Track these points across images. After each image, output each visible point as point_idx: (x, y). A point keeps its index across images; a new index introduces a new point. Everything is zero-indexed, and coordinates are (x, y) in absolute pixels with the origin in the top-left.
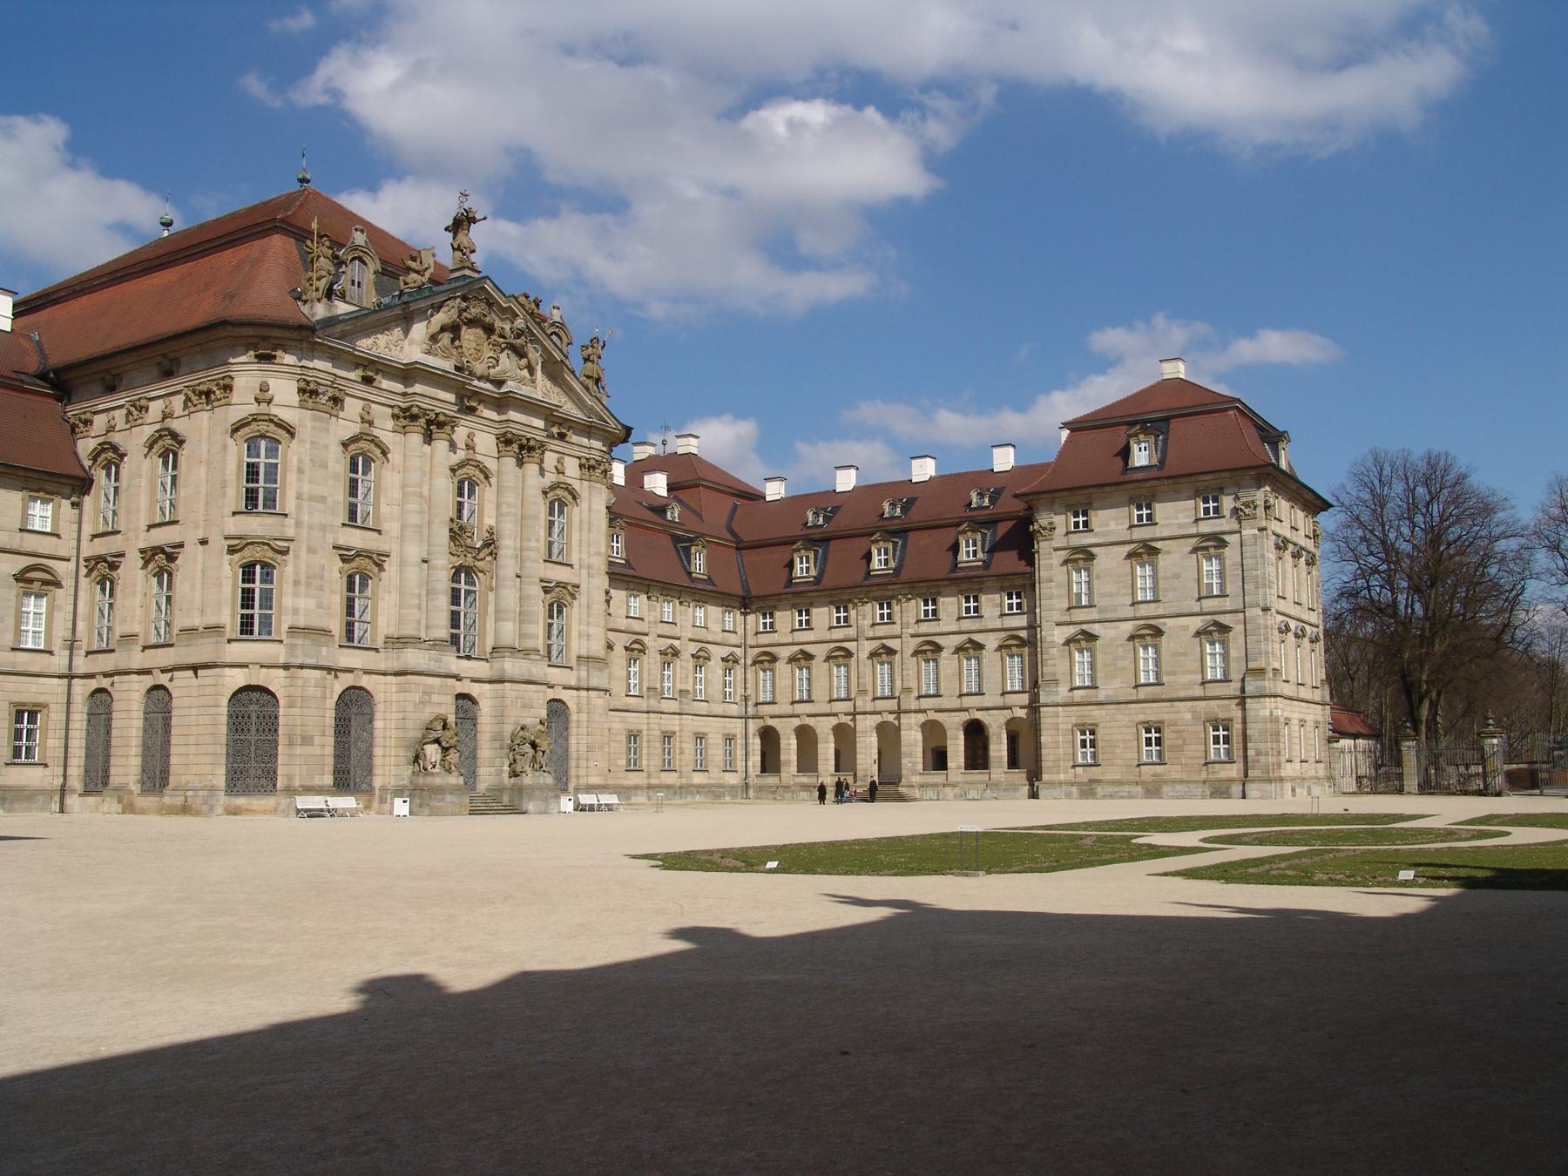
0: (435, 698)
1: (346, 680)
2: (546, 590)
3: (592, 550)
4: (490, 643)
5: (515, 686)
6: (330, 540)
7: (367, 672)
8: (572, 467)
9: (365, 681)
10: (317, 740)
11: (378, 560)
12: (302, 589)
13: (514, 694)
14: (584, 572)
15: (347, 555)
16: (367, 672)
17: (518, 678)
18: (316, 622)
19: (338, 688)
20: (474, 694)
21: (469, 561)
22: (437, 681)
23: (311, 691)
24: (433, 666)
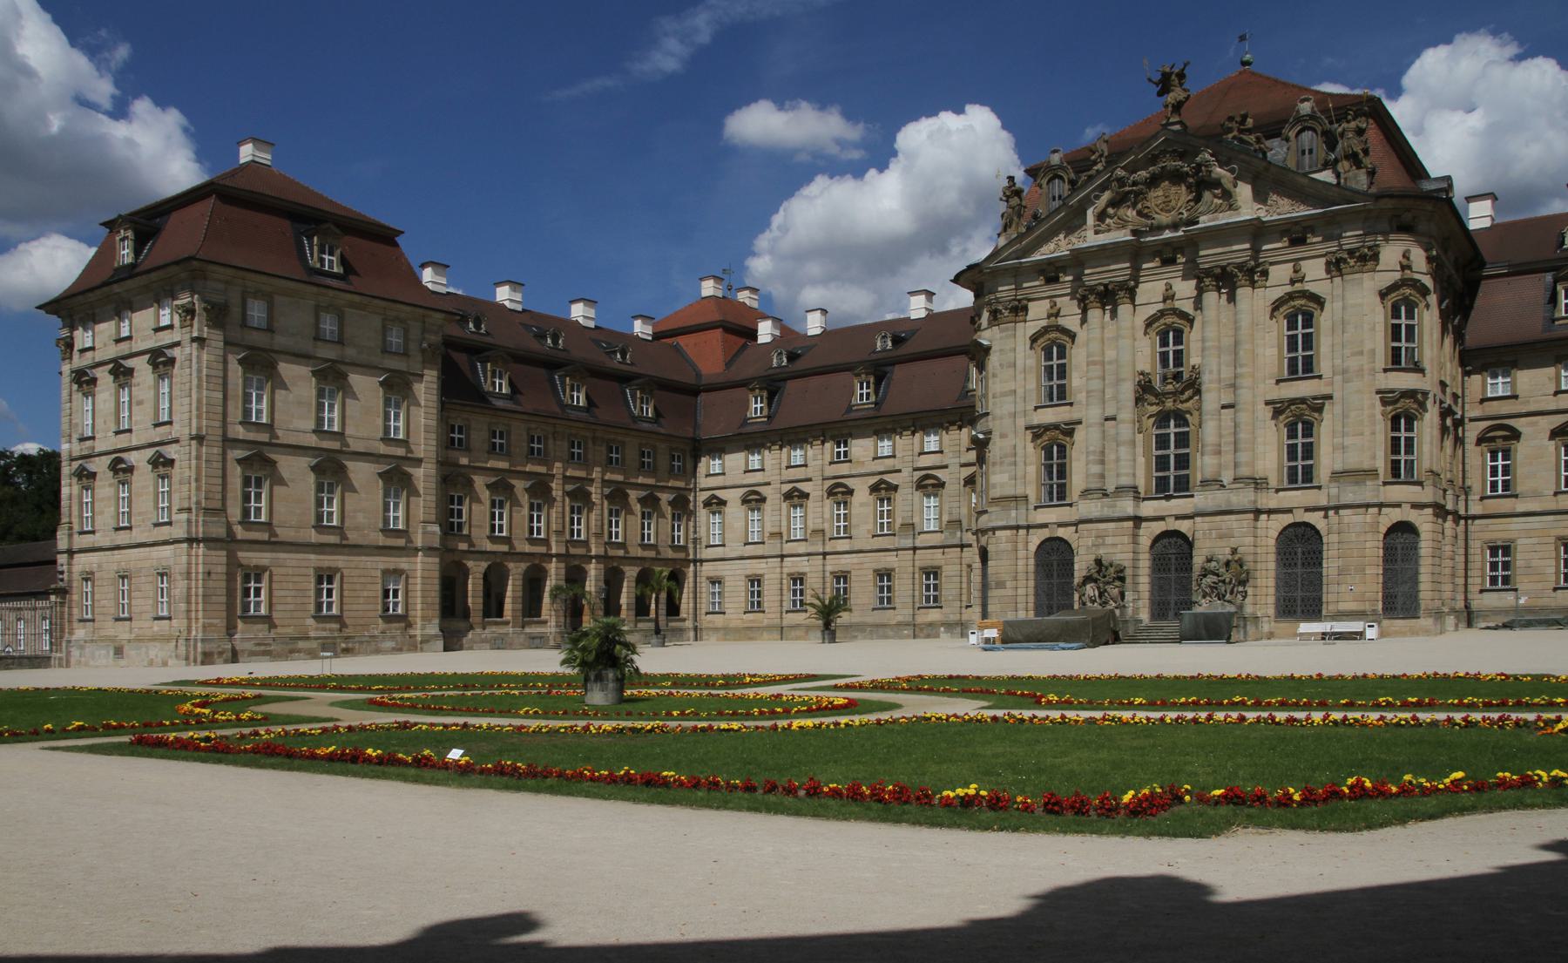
0: (1109, 540)
1: (1045, 534)
2: (1384, 402)
3: (1347, 352)
4: (1199, 478)
5: (1207, 519)
6: (1021, 423)
7: (1061, 525)
8: (1314, 269)
9: (1061, 533)
10: (1008, 584)
11: (1068, 429)
12: (997, 468)
13: (1206, 526)
14: (1338, 378)
15: (1037, 432)
16: (1061, 525)
17: (1210, 510)
18: (1009, 491)
19: (1036, 538)
20: (1183, 530)
21: (1169, 404)
22: (1112, 525)
23: (1003, 546)
24: (1107, 512)
